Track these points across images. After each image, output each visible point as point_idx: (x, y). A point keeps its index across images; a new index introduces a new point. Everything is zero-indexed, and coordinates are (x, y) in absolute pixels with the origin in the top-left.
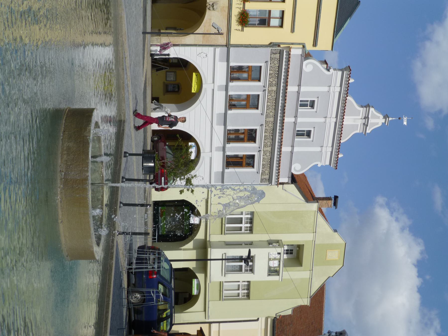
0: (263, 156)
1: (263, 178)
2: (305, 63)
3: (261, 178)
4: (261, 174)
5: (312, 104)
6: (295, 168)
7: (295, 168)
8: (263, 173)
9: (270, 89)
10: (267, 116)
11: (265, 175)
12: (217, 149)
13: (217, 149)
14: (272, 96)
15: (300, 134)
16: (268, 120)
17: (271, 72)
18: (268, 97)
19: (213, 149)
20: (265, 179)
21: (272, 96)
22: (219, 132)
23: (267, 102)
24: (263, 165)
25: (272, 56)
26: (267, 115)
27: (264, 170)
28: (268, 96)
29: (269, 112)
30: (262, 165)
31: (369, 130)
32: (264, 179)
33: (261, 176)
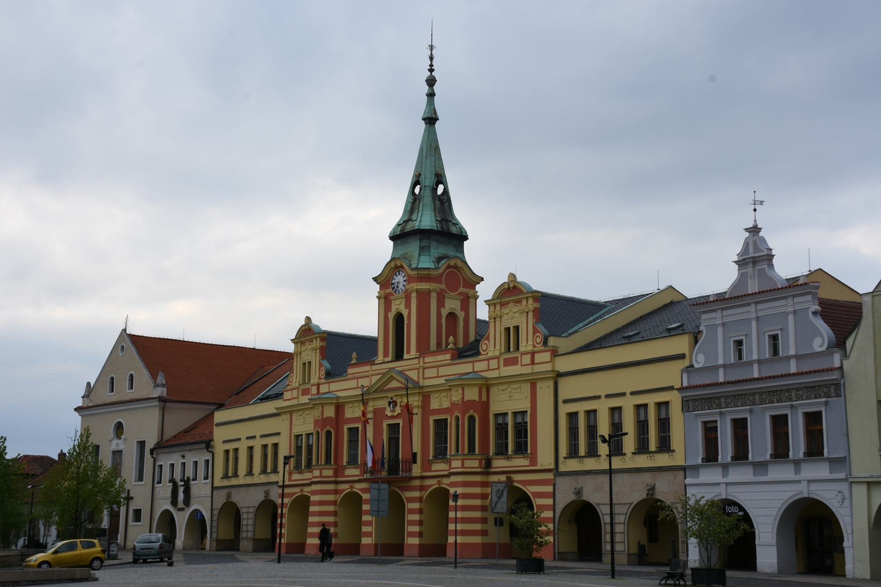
0: (803, 400)
1: (833, 395)
2: (696, 366)
3: (835, 397)
4: (829, 398)
5: (739, 343)
6: (820, 346)
7: (820, 346)
8: (827, 396)
9: (724, 406)
10: (754, 404)
11: (830, 391)
12: (797, 471)
13: (797, 471)
14: (732, 401)
15: (775, 351)
16: (758, 402)
17: (706, 407)
18: (733, 406)
19: (797, 478)
20: (836, 390)
21: (732, 401)
22: (781, 472)
23: (738, 407)
24: (816, 398)
25: (691, 409)
26: (752, 404)
27: (823, 394)
28: (731, 407)
29: (749, 402)
30: (816, 399)
31: (763, 251)
32: (837, 391)
33: (832, 397)
